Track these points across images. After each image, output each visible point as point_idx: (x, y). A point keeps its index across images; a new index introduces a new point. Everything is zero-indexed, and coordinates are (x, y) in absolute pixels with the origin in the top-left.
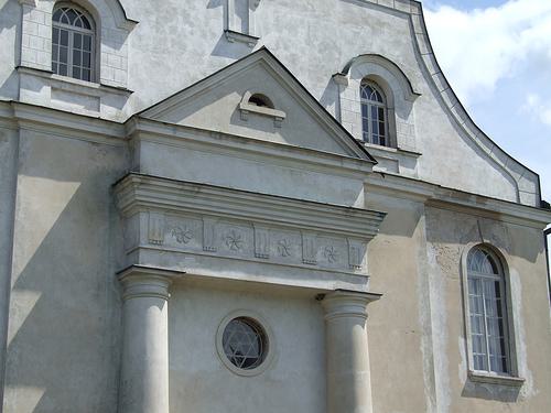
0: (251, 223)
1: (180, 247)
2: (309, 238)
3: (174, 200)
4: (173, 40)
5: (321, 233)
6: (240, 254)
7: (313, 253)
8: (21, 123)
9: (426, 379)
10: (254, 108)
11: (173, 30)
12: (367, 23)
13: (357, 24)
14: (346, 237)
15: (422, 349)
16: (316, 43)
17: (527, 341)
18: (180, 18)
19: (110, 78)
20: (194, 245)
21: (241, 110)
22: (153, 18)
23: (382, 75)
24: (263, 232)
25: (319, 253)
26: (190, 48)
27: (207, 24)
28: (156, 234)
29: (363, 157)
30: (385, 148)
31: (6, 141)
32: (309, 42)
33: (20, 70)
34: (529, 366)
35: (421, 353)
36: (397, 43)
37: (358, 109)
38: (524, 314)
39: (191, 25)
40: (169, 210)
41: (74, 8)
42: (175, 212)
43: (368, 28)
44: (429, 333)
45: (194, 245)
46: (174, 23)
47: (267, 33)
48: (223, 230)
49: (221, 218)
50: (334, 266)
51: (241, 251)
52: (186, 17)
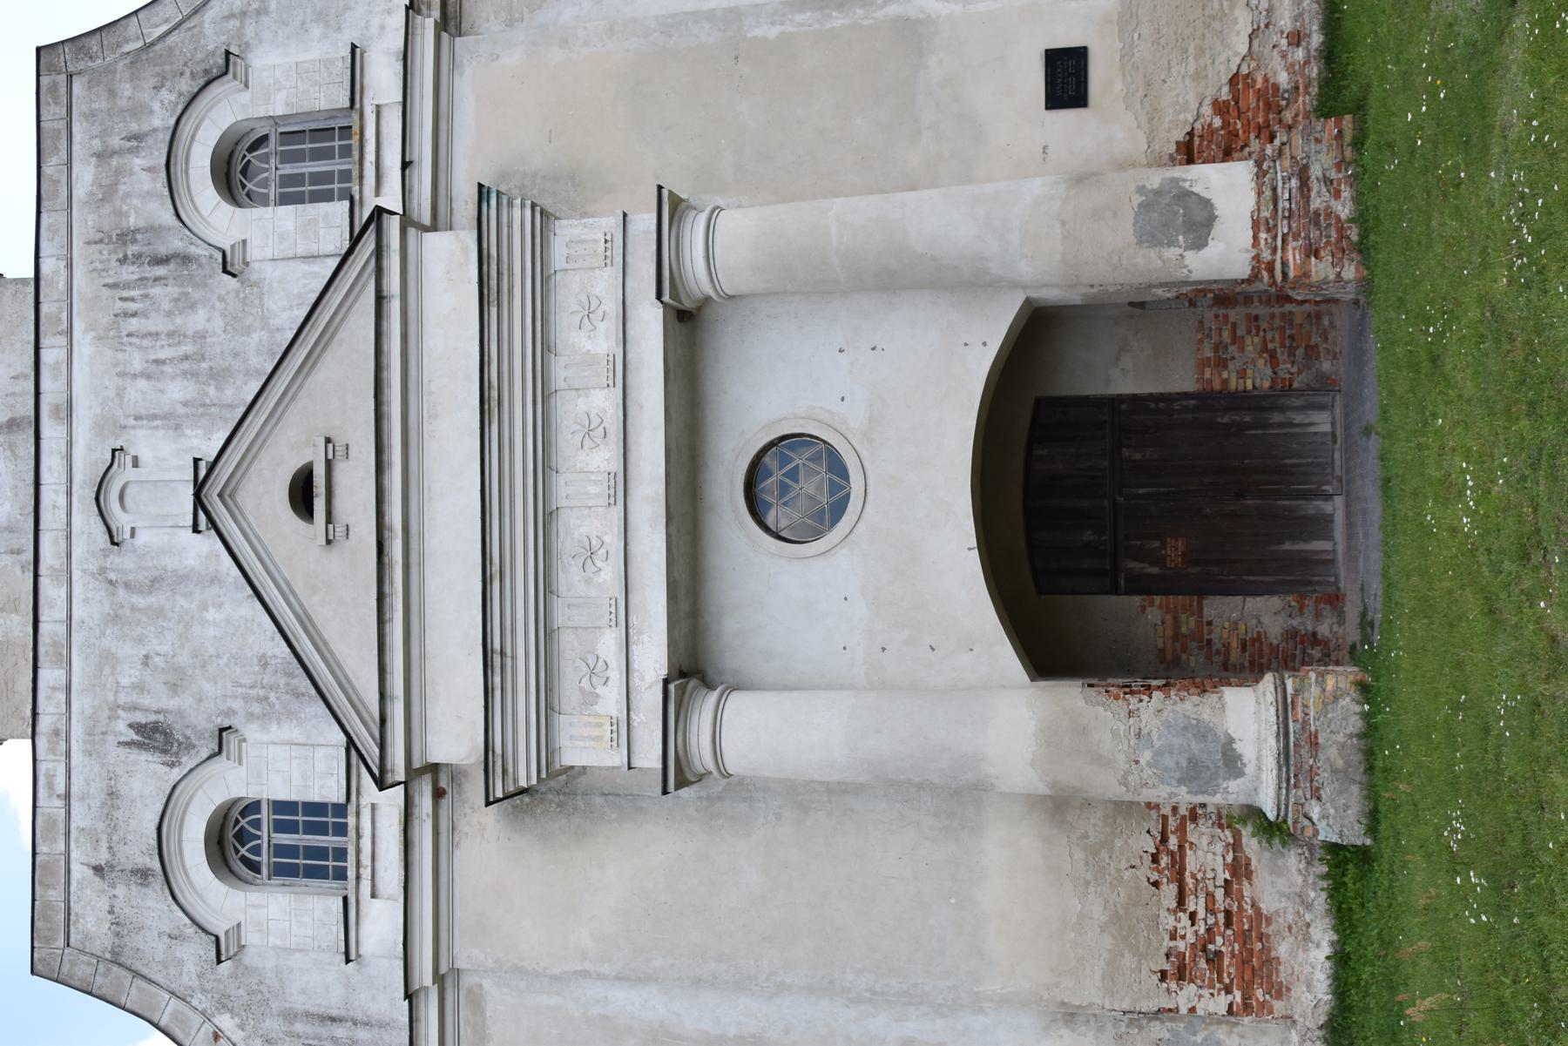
0: (546, 518)
1: (616, 675)
2: (561, 372)
3: (523, 703)
5: (544, 345)
6: (613, 541)
7: (590, 360)
8: (443, 970)
14: (546, 280)
15: (773, 33)
20: (608, 646)
21: (329, 542)
23: (207, 162)
24: (564, 489)
25: (588, 345)
28: (596, 732)
29: (368, 245)
30: (356, 128)
31: (481, 986)
33: (353, 956)
35: (782, 33)
37: (287, 216)
40: (548, 707)
41: (230, 834)
42: (548, 690)
48: (570, 577)
49: (546, 586)
50: (612, 306)
51: (607, 539)
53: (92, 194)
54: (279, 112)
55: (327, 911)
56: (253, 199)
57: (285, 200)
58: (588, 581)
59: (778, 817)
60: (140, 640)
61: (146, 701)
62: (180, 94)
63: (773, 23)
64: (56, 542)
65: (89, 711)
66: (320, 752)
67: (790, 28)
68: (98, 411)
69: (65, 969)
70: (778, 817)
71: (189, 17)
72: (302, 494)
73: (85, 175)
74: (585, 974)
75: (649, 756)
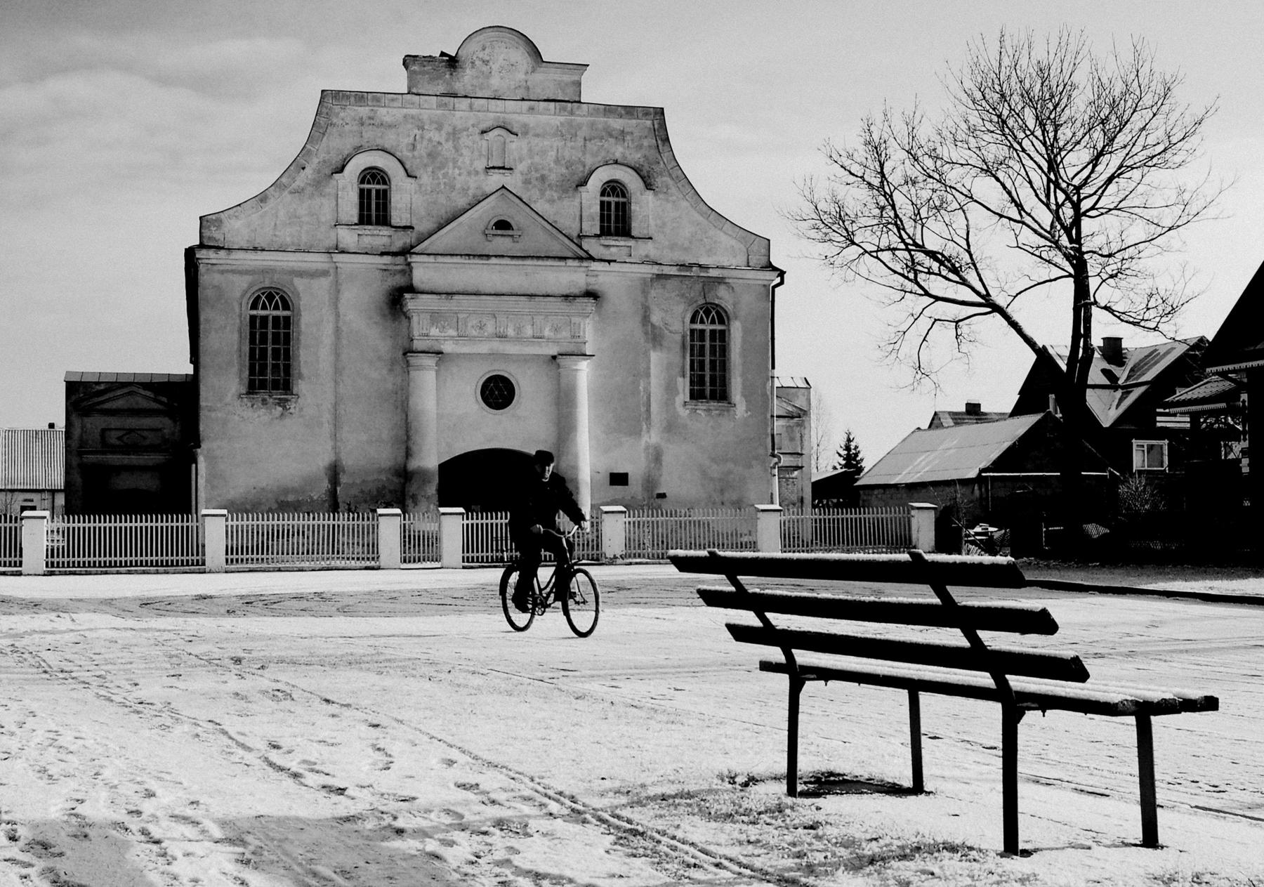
4: (445, 183)
9: (643, 409)
10: (499, 232)
11: (445, 175)
12: (611, 135)
13: (602, 138)
16: (563, 162)
17: (743, 375)
18: (451, 165)
19: (398, 220)
20: (452, 332)
22: (430, 169)
25: (547, 329)
26: (458, 186)
27: (471, 164)
32: (557, 161)
34: (744, 395)
36: (640, 147)
38: (744, 354)
39: (460, 168)
43: (612, 140)
44: (648, 375)
45: (452, 332)
46: (446, 169)
47: (521, 162)
52: (455, 161)
53: (609, 127)
54: (632, 208)
55: (352, 216)
56: (603, 194)
57: (602, 203)
58: (473, 327)
59: (394, 384)
60: (447, 140)
61: (425, 142)
62: (642, 166)
63: (644, 388)
64: (483, 106)
65: (421, 117)
66: (409, 216)
67: (642, 394)
68: (531, 125)
69: (325, 104)
70: (394, 384)
71: (668, 171)
72: (503, 225)
73: (617, 123)
74: (338, 315)
75: (418, 345)
